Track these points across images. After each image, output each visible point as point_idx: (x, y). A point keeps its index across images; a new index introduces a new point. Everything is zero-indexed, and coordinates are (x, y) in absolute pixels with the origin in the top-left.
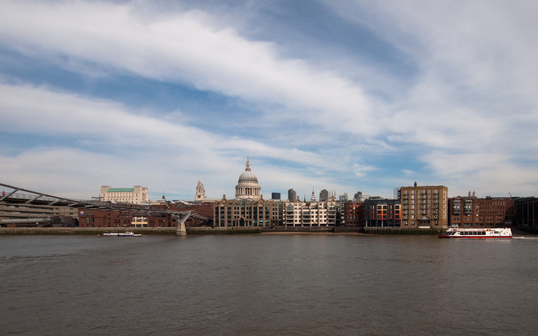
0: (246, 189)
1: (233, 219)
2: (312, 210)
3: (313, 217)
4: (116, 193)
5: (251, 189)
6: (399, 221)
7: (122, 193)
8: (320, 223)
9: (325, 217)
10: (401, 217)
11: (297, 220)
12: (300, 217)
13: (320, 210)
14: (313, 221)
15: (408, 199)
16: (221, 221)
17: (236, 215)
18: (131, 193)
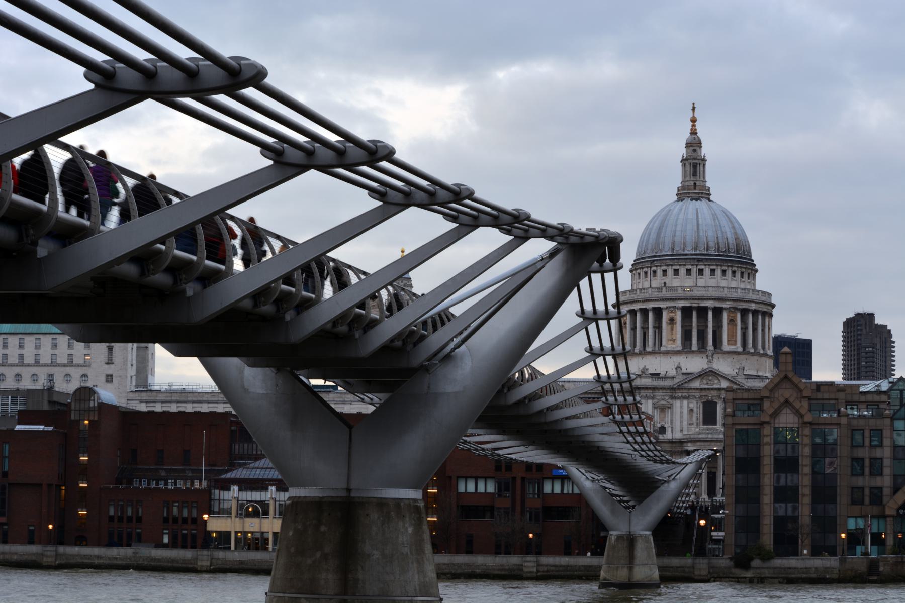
0: (686, 312)
5: (718, 311)
16: (779, 522)
17: (865, 482)
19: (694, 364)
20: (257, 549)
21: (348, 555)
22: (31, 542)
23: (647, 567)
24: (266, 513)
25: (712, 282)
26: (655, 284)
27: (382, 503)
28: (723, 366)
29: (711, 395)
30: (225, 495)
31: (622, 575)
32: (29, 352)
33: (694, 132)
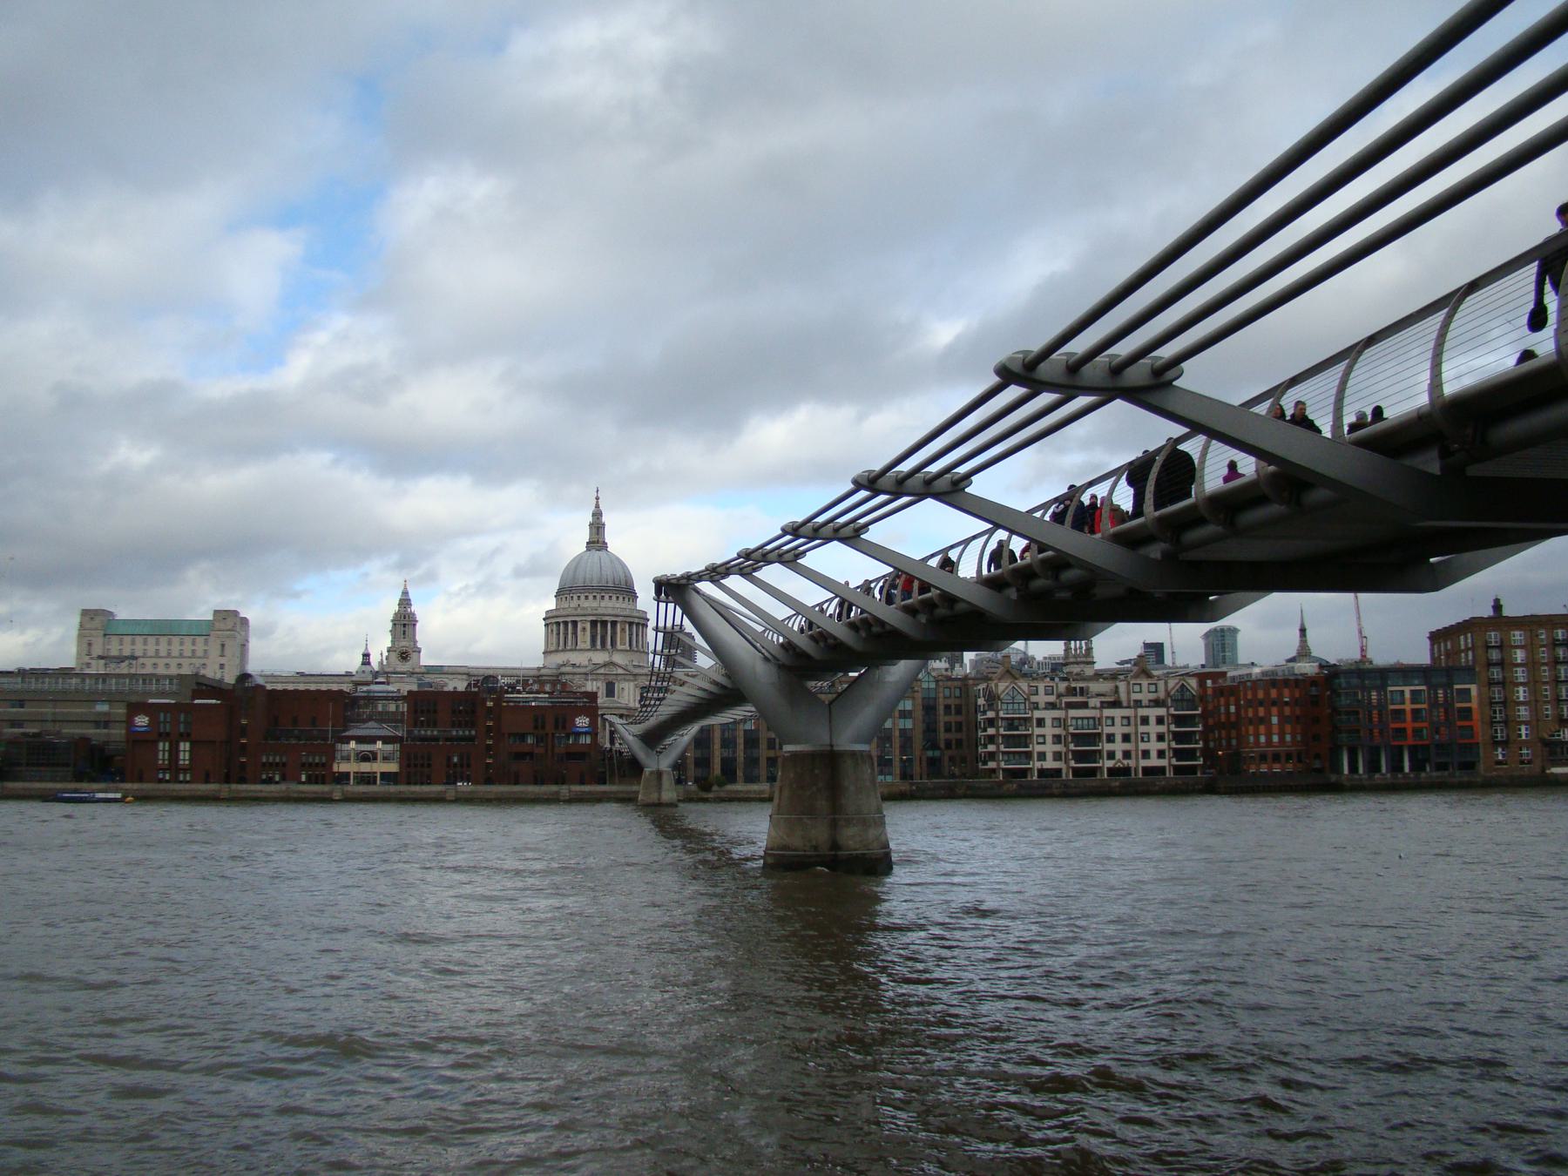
0: (594, 623)
1: (764, 752)
2: (1107, 712)
3: (1111, 738)
4: (139, 640)
5: (614, 623)
6: (1472, 748)
7: (164, 640)
8: (1144, 763)
9: (1160, 738)
10: (1481, 734)
11: (1047, 751)
12: (1057, 739)
13: (1142, 712)
14: (1111, 755)
15: (1501, 664)
18: (200, 640)
19: (600, 657)
20: (368, 783)
21: (834, 789)
22: (207, 781)
23: (669, 793)
24: (375, 758)
25: (610, 604)
26: (574, 603)
27: (853, 754)
28: (618, 658)
29: (611, 678)
30: (345, 747)
31: (654, 797)
32: (176, 649)
33: (597, 506)
